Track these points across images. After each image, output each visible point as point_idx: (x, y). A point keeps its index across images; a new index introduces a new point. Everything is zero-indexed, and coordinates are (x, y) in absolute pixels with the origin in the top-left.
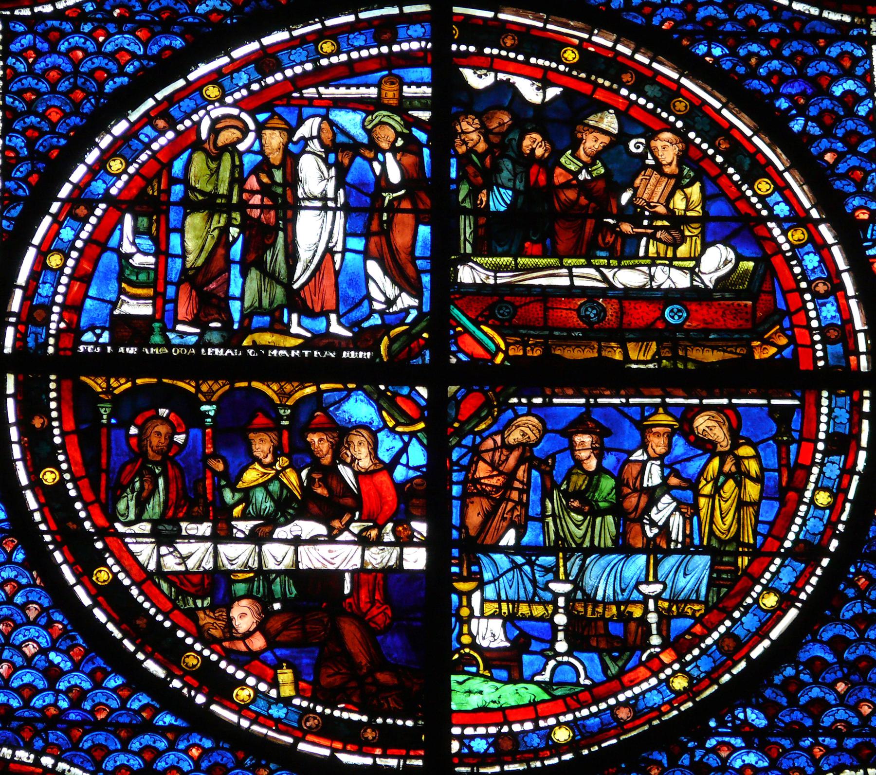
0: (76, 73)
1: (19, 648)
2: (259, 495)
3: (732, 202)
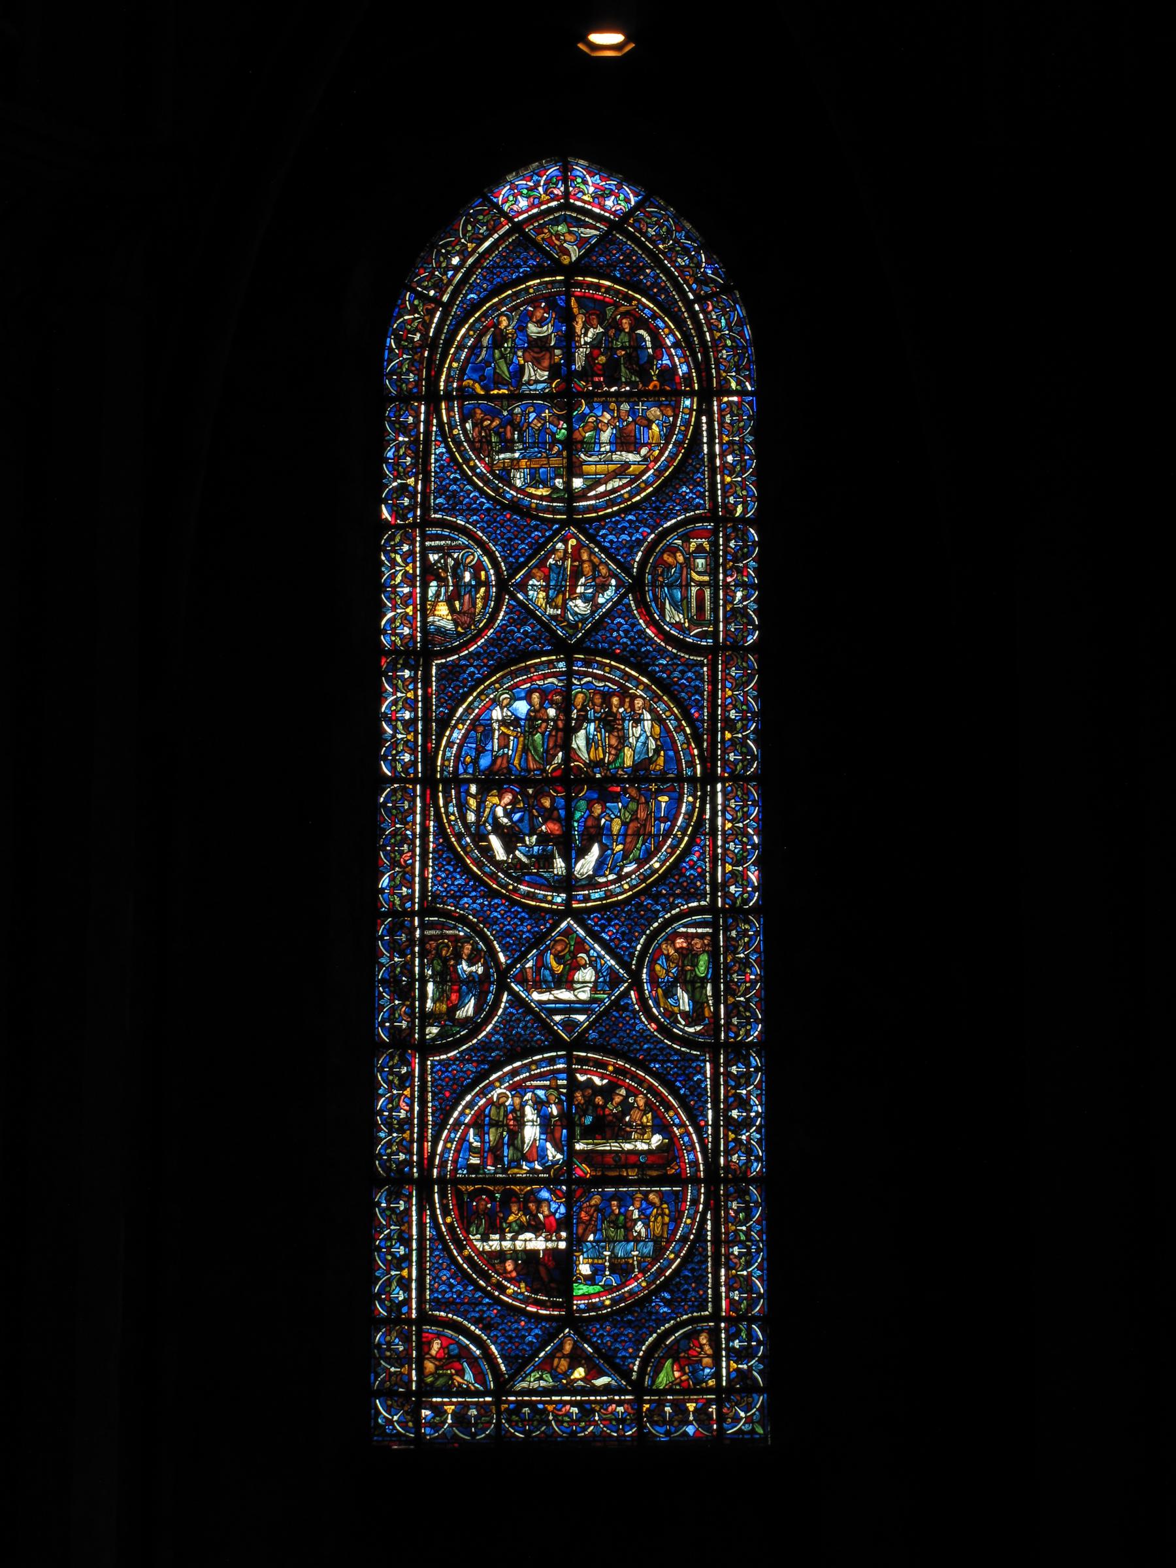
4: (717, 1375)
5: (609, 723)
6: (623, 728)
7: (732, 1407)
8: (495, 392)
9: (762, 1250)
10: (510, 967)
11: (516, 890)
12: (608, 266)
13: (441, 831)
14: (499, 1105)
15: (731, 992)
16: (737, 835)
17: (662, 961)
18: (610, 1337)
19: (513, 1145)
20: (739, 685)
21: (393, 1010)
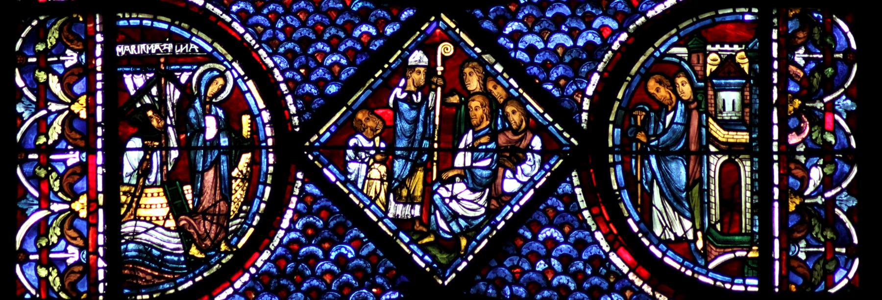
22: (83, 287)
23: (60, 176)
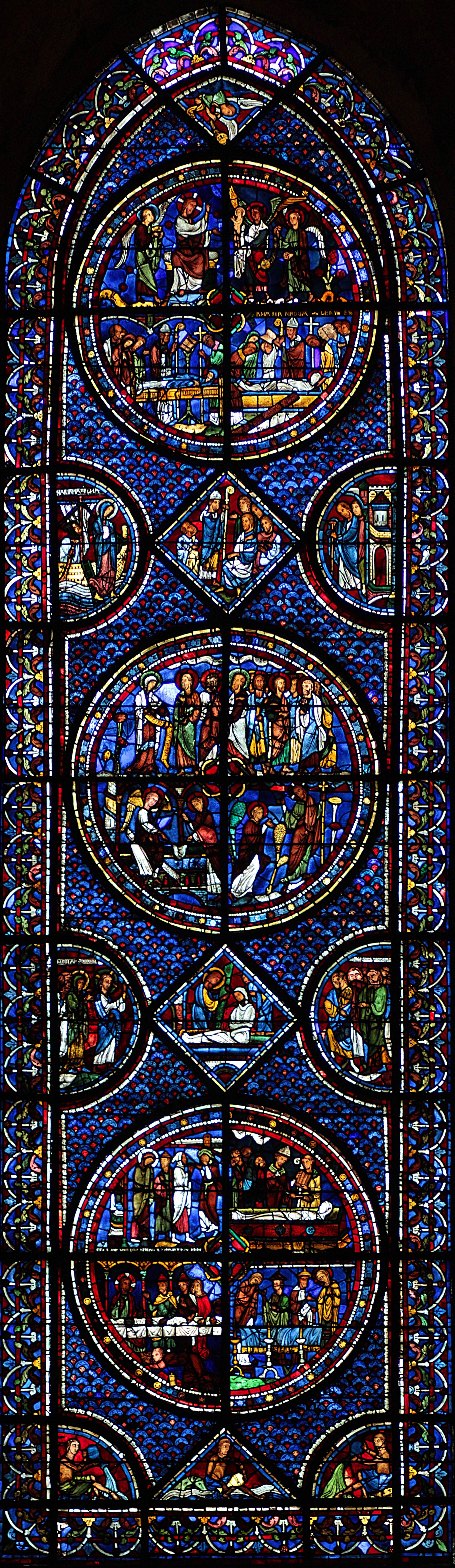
0: (93, 1136)
1: (78, 1370)
2: (162, 1307)
3: (331, 1184)
4: (394, 1483)
5: (272, 709)
6: (289, 717)
7: (412, 1520)
8: (139, 304)
9: (446, 1338)
10: (156, 1003)
11: (163, 910)
12: (273, 145)
13: (75, 838)
14: (144, 1168)
15: (412, 1032)
16: (421, 844)
17: (333, 995)
18: (272, 1436)
19: (161, 1214)
20: (424, 664)
21: (20, 1054)
22: (39, 616)
23: (27, 558)
